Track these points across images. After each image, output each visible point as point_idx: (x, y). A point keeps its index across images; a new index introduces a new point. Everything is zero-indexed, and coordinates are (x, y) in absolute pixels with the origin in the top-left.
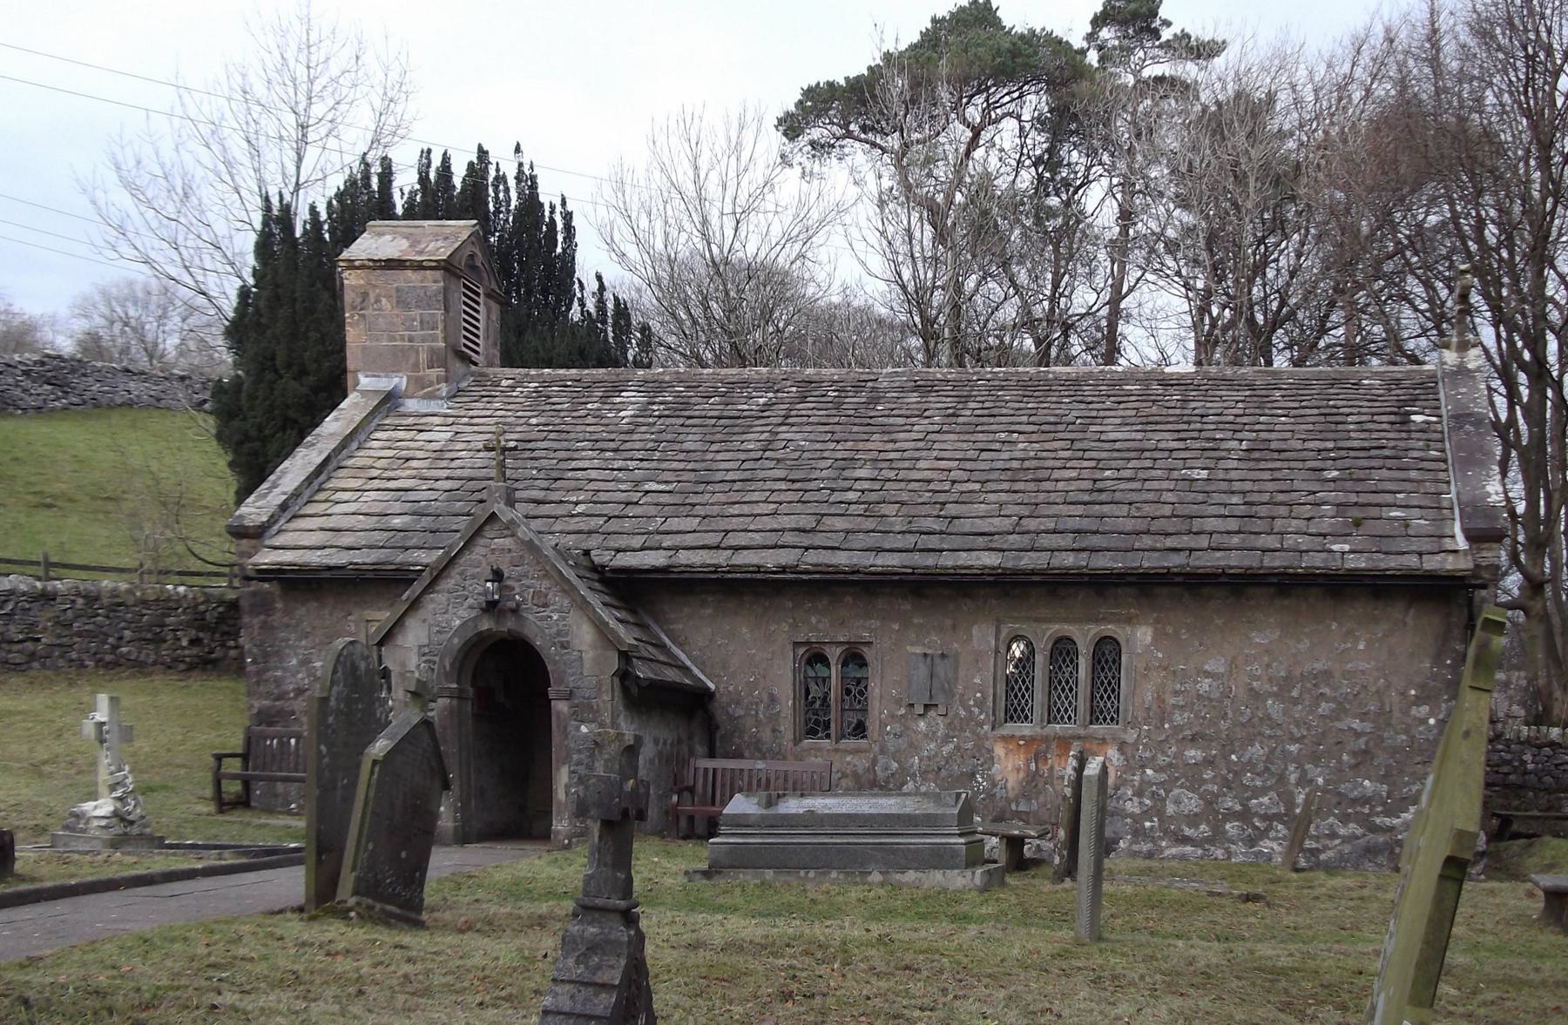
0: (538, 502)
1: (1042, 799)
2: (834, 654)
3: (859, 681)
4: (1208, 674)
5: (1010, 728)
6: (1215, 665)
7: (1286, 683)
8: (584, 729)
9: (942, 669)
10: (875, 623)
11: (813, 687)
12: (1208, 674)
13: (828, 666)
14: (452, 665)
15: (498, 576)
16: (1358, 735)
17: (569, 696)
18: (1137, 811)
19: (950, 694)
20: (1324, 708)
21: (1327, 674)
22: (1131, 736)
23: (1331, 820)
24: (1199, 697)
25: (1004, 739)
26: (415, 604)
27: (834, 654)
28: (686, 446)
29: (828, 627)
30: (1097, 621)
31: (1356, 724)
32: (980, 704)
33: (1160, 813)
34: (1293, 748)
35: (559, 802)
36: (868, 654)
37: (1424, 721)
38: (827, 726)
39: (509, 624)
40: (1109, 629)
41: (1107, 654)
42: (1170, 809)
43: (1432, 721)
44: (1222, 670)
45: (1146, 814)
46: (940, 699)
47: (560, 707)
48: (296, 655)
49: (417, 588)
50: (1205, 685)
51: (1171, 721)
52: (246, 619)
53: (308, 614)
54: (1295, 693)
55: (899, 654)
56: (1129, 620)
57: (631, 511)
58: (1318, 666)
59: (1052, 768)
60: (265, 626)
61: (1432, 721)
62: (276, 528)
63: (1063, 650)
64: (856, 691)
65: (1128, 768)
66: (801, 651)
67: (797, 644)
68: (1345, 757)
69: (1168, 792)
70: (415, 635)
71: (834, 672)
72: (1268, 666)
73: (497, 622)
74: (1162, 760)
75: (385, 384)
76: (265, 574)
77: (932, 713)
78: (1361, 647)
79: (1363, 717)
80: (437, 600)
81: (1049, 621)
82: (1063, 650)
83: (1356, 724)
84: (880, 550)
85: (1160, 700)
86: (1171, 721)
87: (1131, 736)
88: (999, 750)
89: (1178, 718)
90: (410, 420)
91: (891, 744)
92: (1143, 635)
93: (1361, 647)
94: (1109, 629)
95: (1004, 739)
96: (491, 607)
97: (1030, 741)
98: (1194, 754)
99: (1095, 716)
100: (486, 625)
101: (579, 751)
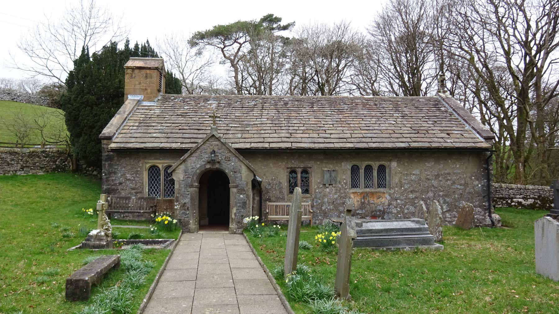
0: (199, 130)
1: (366, 209)
2: (299, 171)
3: (306, 178)
4: (414, 174)
6: (416, 172)
7: (437, 176)
8: (241, 196)
9: (333, 174)
11: (292, 180)
12: (414, 174)
13: (296, 174)
14: (196, 178)
15: (214, 152)
17: (236, 187)
18: (396, 212)
19: (336, 181)
21: (449, 174)
23: (454, 213)
24: (412, 180)
25: (353, 193)
26: (184, 161)
27: (299, 171)
28: (237, 115)
30: (379, 161)
31: (459, 187)
32: (346, 184)
33: (403, 212)
34: (441, 193)
35: (232, 219)
37: (478, 185)
39: (217, 166)
40: (370, 163)
41: (382, 169)
42: (406, 211)
43: (480, 185)
44: (418, 173)
45: (398, 212)
46: (333, 182)
47: (233, 191)
48: (120, 173)
49: (186, 155)
50: (413, 177)
51: (404, 187)
52: (103, 162)
53: (124, 162)
54: (440, 179)
56: (390, 161)
57: (228, 132)
58: (446, 172)
59: (369, 201)
60: (110, 165)
61: (480, 185)
62: (115, 137)
63: (368, 169)
66: (289, 170)
67: (288, 168)
68: (456, 196)
69: (405, 206)
71: (299, 176)
72: (431, 172)
73: (213, 166)
75: (138, 97)
76: (113, 150)
77: (331, 186)
78: (458, 166)
79: (461, 185)
80: (193, 159)
81: (366, 161)
82: (368, 169)
83: (459, 187)
84: (314, 143)
85: (400, 181)
86: (404, 187)
87: (392, 191)
88: (352, 196)
89: (406, 187)
90: (146, 107)
91: (318, 196)
92: (394, 164)
93: (458, 166)
94: (370, 163)
96: (212, 162)
97: (361, 193)
98: (411, 196)
99: (379, 186)
100: (208, 166)
101: (240, 203)
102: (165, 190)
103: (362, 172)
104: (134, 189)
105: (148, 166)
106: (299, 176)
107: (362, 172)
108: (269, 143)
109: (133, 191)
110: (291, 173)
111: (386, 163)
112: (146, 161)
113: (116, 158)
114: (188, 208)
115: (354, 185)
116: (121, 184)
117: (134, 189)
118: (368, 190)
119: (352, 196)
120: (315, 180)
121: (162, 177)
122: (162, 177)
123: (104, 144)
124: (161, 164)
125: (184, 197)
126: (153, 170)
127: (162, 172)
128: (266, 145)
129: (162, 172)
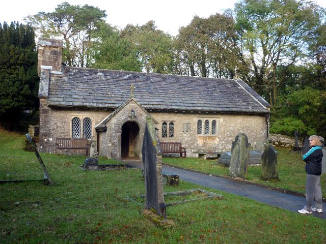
2: (168, 123)
5: (199, 135)
10: (176, 118)
16: (253, 135)
20: (249, 131)
22: (220, 136)
25: (200, 137)
26: (114, 115)
27: (168, 123)
29: (167, 118)
36: (174, 123)
38: (166, 135)
39: (134, 119)
41: (214, 123)
42: (227, 148)
50: (231, 128)
52: (41, 114)
55: (180, 121)
63: (207, 122)
64: (172, 129)
65: (220, 141)
70: (114, 121)
71: (168, 126)
74: (225, 140)
82: (207, 122)
85: (224, 131)
88: (198, 139)
95: (200, 137)
97: (204, 137)
100: (129, 119)
102: (84, 134)
103: (203, 124)
104: (63, 133)
105: (73, 117)
106: (168, 126)
107: (203, 124)
108: (152, 105)
109: (63, 135)
110: (163, 124)
111: (217, 120)
112: (72, 114)
113: (50, 112)
114: (116, 146)
115: (199, 132)
116: (53, 129)
117: (63, 133)
118: (206, 135)
119: (198, 139)
120: (177, 129)
121: (82, 125)
122: (82, 125)
123: (41, 102)
124: (82, 116)
125: (115, 139)
126: (76, 121)
127: (82, 122)
128: (151, 106)
129: (82, 122)
